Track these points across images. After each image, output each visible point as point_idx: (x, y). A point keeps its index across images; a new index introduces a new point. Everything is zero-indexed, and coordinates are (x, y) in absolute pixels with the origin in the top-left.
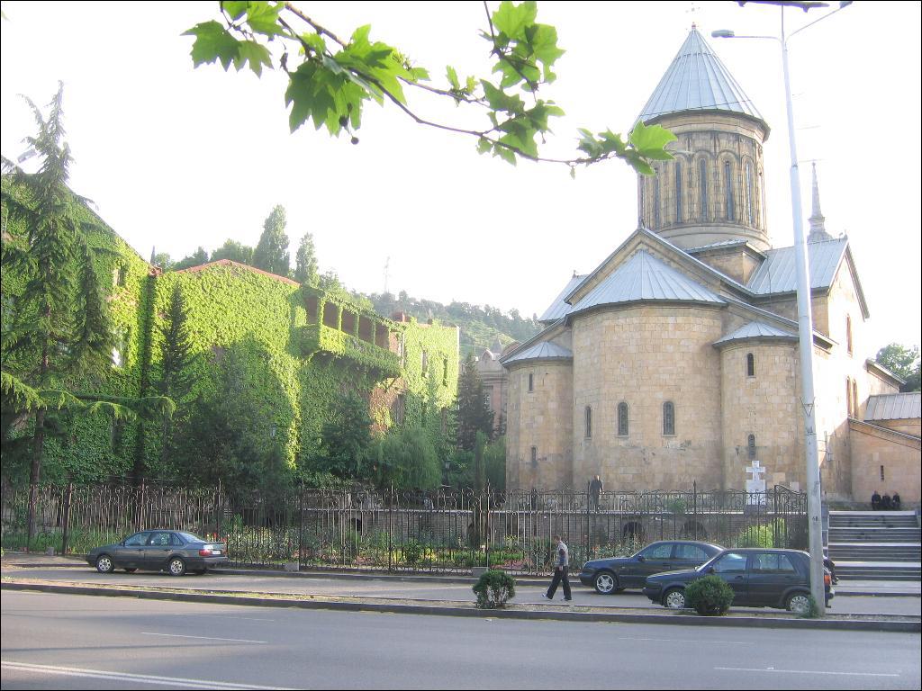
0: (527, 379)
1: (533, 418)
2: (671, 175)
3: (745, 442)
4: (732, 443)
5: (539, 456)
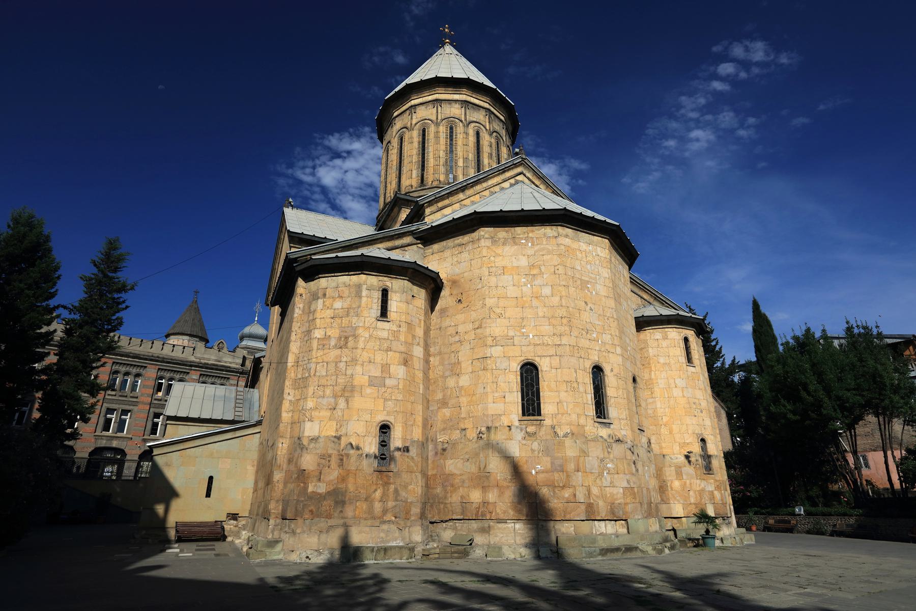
0: (378, 295)
1: (385, 368)
2: (472, 139)
3: (696, 448)
4: (676, 448)
5: (397, 440)
